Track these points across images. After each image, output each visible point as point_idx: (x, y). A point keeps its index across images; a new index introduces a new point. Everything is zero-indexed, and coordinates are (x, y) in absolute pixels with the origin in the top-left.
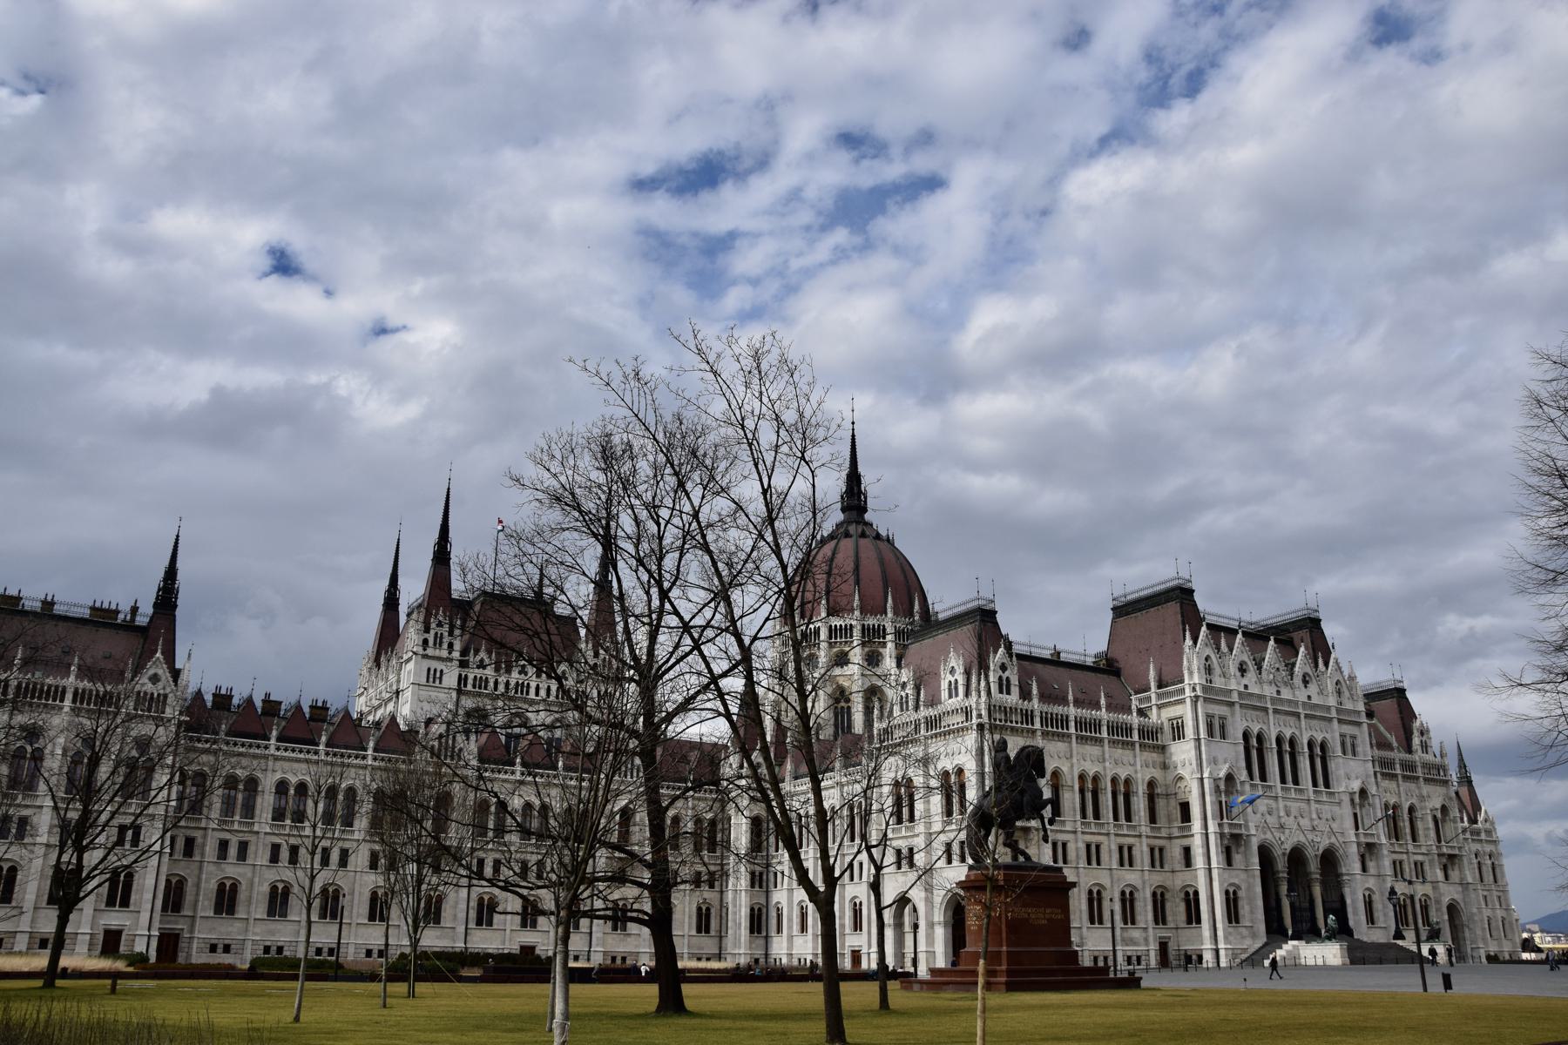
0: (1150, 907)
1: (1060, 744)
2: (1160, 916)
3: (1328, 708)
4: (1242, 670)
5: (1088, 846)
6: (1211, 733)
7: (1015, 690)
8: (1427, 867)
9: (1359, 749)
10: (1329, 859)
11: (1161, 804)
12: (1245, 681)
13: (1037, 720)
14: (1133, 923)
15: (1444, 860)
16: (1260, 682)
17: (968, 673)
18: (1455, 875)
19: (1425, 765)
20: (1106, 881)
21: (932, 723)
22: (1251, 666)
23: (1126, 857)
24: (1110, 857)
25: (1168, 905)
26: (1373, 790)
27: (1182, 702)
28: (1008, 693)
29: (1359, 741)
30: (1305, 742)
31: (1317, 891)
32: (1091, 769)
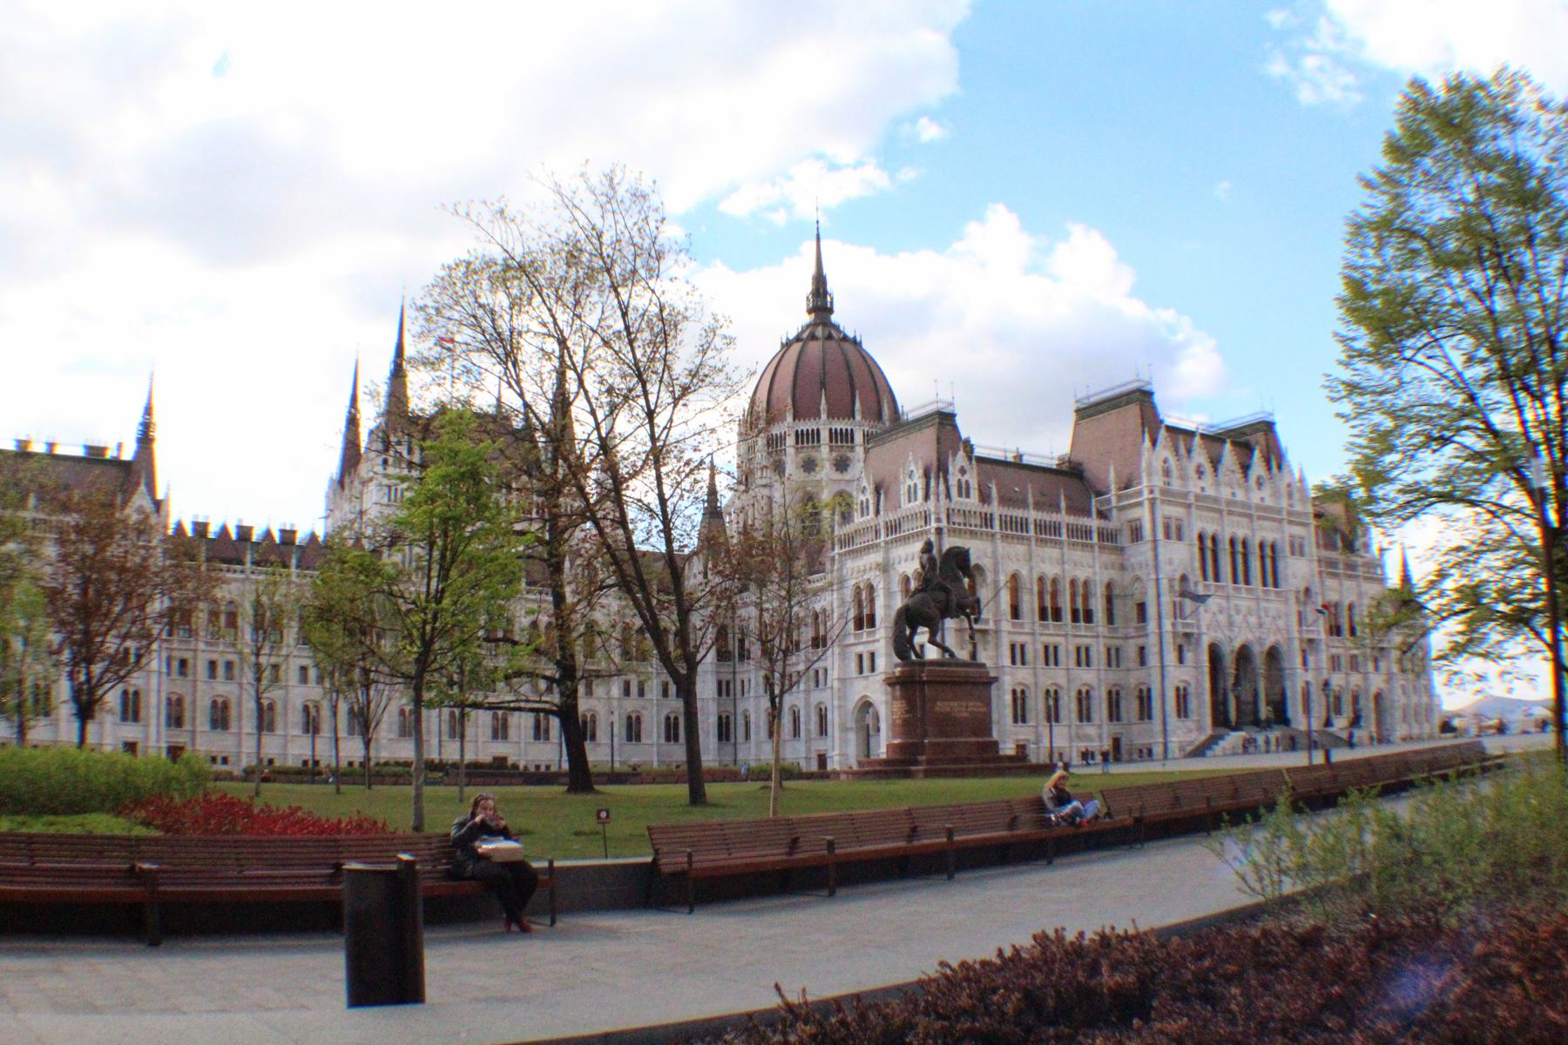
0: (1105, 705)
2: (1114, 713)
3: (1279, 511)
4: (1200, 472)
5: (1046, 648)
6: (1167, 536)
7: (974, 493)
9: (1306, 550)
10: (1273, 654)
12: (1202, 484)
13: (997, 523)
16: (1217, 484)
17: (927, 475)
18: (1382, 665)
19: (1366, 565)
20: (1062, 681)
21: (893, 528)
22: (1208, 468)
23: (1083, 657)
24: (1067, 657)
25: (1123, 704)
26: (1316, 588)
27: (1140, 504)
28: (968, 496)
30: (1257, 542)
31: (1262, 685)
32: (1051, 570)
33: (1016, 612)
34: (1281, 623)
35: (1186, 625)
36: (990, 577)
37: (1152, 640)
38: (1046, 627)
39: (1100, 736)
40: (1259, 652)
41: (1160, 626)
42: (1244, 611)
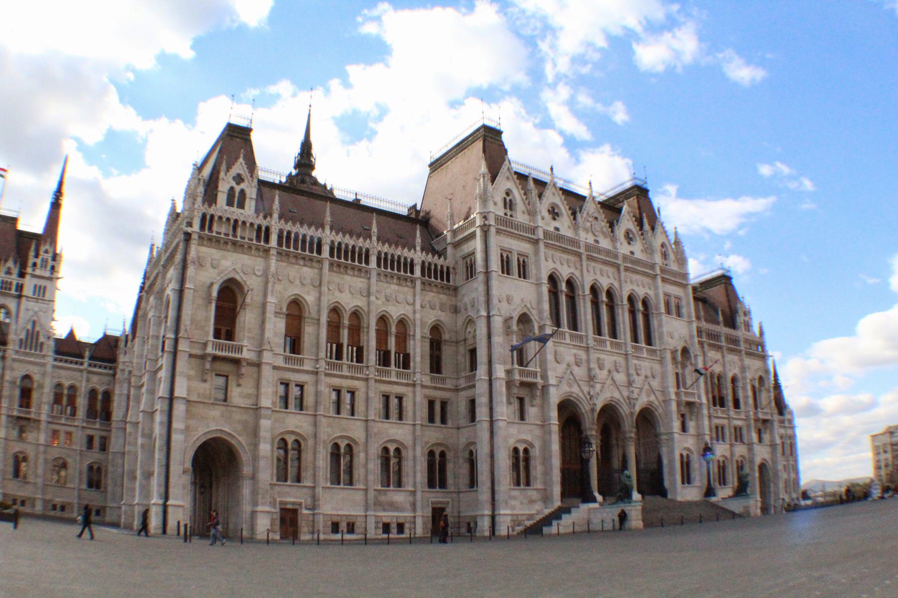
1: (305, 269)
3: (652, 266)
7: (250, 205)
8: (744, 432)
10: (647, 419)
11: (447, 352)
14: (399, 484)
15: (760, 425)
16: (576, 227)
18: (766, 437)
19: (747, 341)
23: (393, 408)
25: (450, 467)
26: (695, 349)
28: (241, 205)
29: (684, 303)
32: (349, 302)
33: (295, 344)
34: (655, 384)
35: (529, 374)
36: (252, 298)
37: (481, 388)
38: (340, 368)
39: (414, 505)
40: (628, 414)
41: (490, 373)
42: (608, 365)
